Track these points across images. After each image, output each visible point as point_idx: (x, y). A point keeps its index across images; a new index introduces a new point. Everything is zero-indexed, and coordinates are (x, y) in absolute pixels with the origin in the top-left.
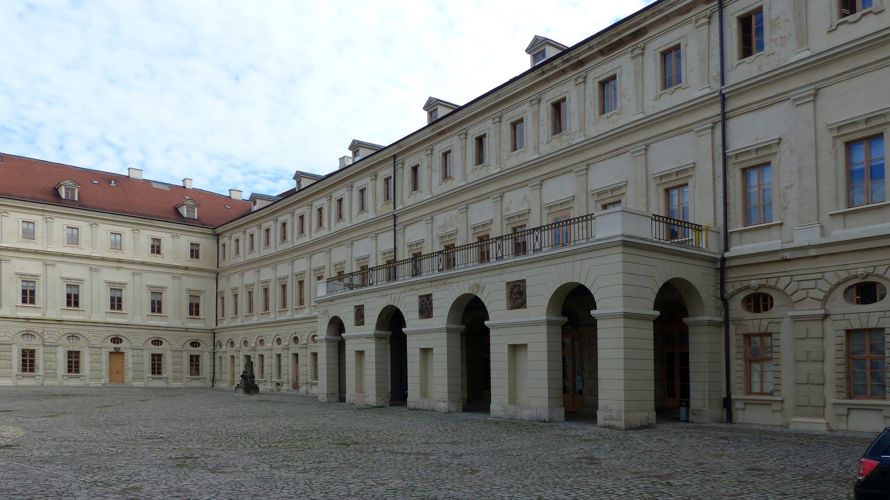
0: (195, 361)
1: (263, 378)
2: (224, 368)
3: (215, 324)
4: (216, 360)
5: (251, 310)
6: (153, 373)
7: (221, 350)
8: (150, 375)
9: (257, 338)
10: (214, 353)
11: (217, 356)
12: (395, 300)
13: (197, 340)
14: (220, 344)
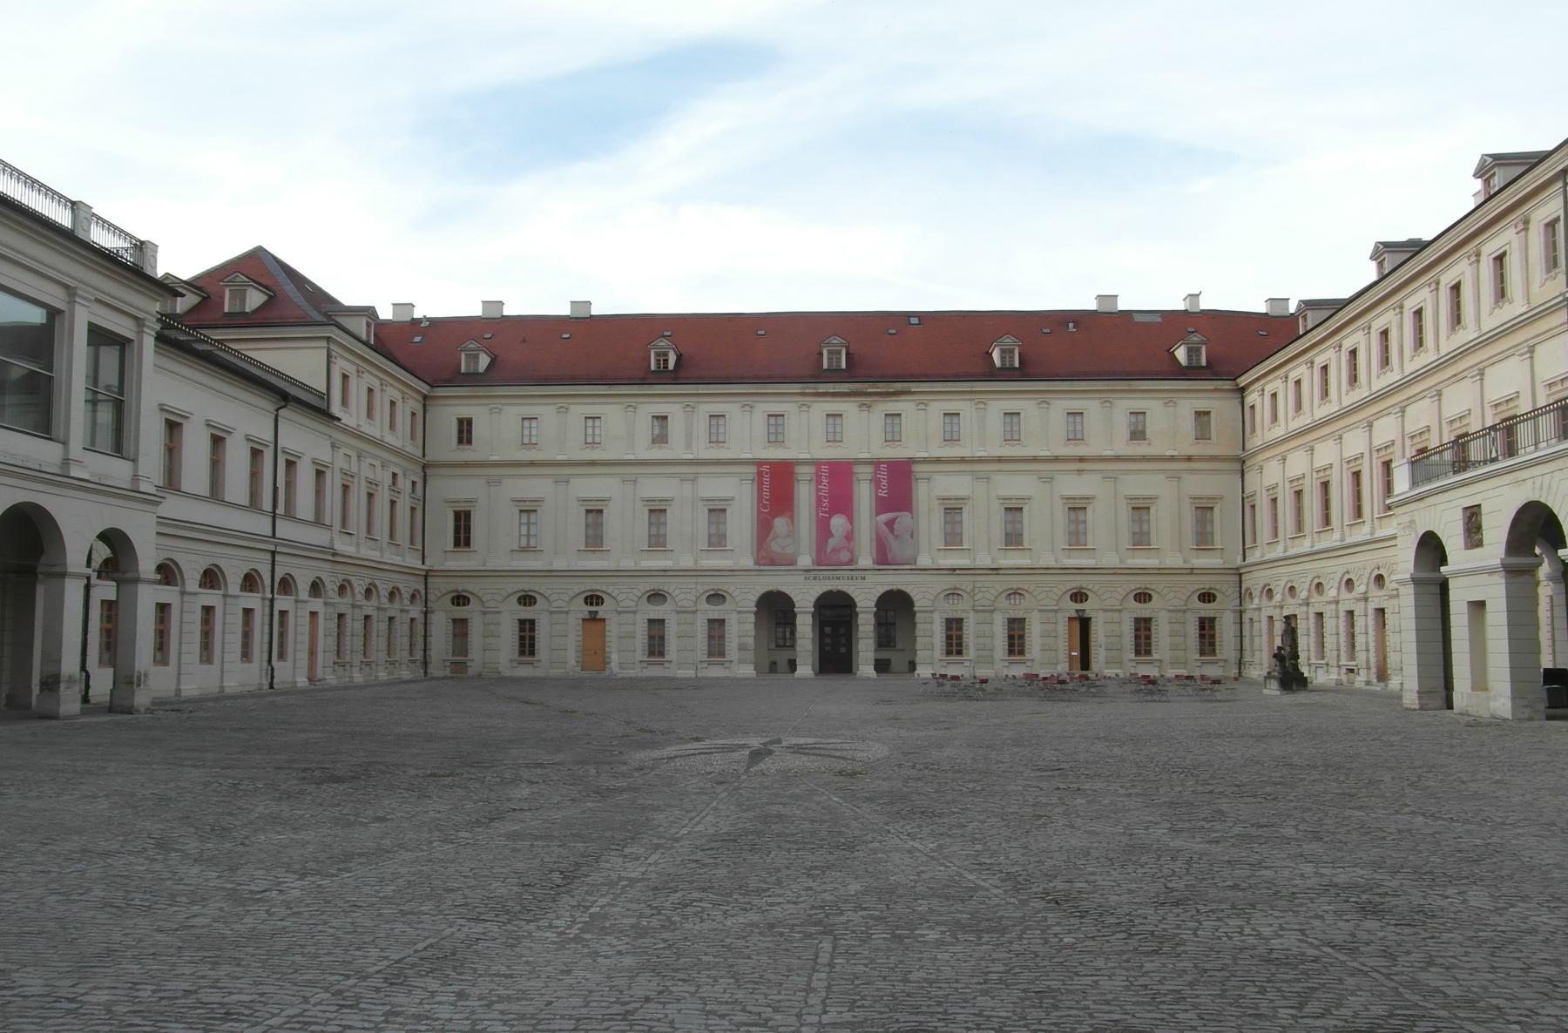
0: (1207, 628)
1: (1323, 658)
2: (1257, 640)
3: (1240, 557)
4: (1244, 625)
5: (1299, 526)
6: (1138, 653)
7: (1252, 606)
8: (1132, 656)
9: (1312, 581)
10: (1241, 613)
11: (1246, 617)
12: (1541, 488)
13: (1211, 589)
14: (1251, 594)
